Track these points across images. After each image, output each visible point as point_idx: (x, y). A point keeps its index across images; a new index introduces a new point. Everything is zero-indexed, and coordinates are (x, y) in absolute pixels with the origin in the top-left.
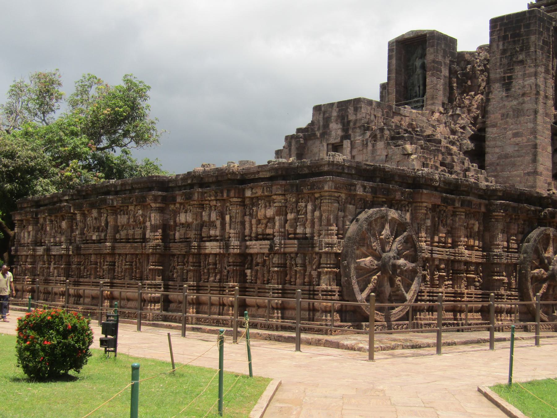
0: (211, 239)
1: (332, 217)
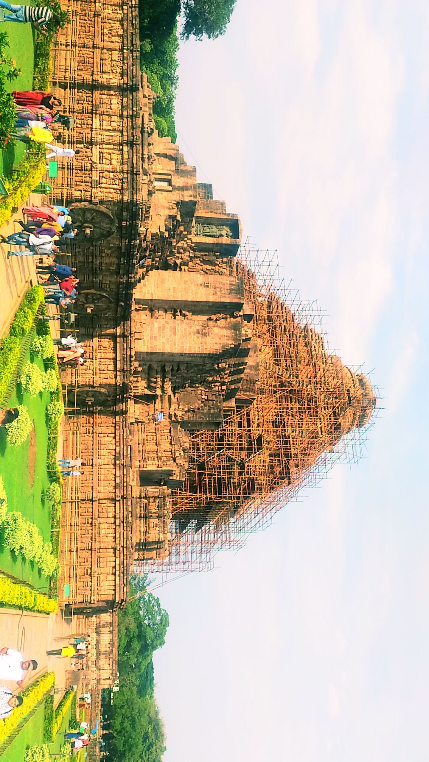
1: (110, 199)
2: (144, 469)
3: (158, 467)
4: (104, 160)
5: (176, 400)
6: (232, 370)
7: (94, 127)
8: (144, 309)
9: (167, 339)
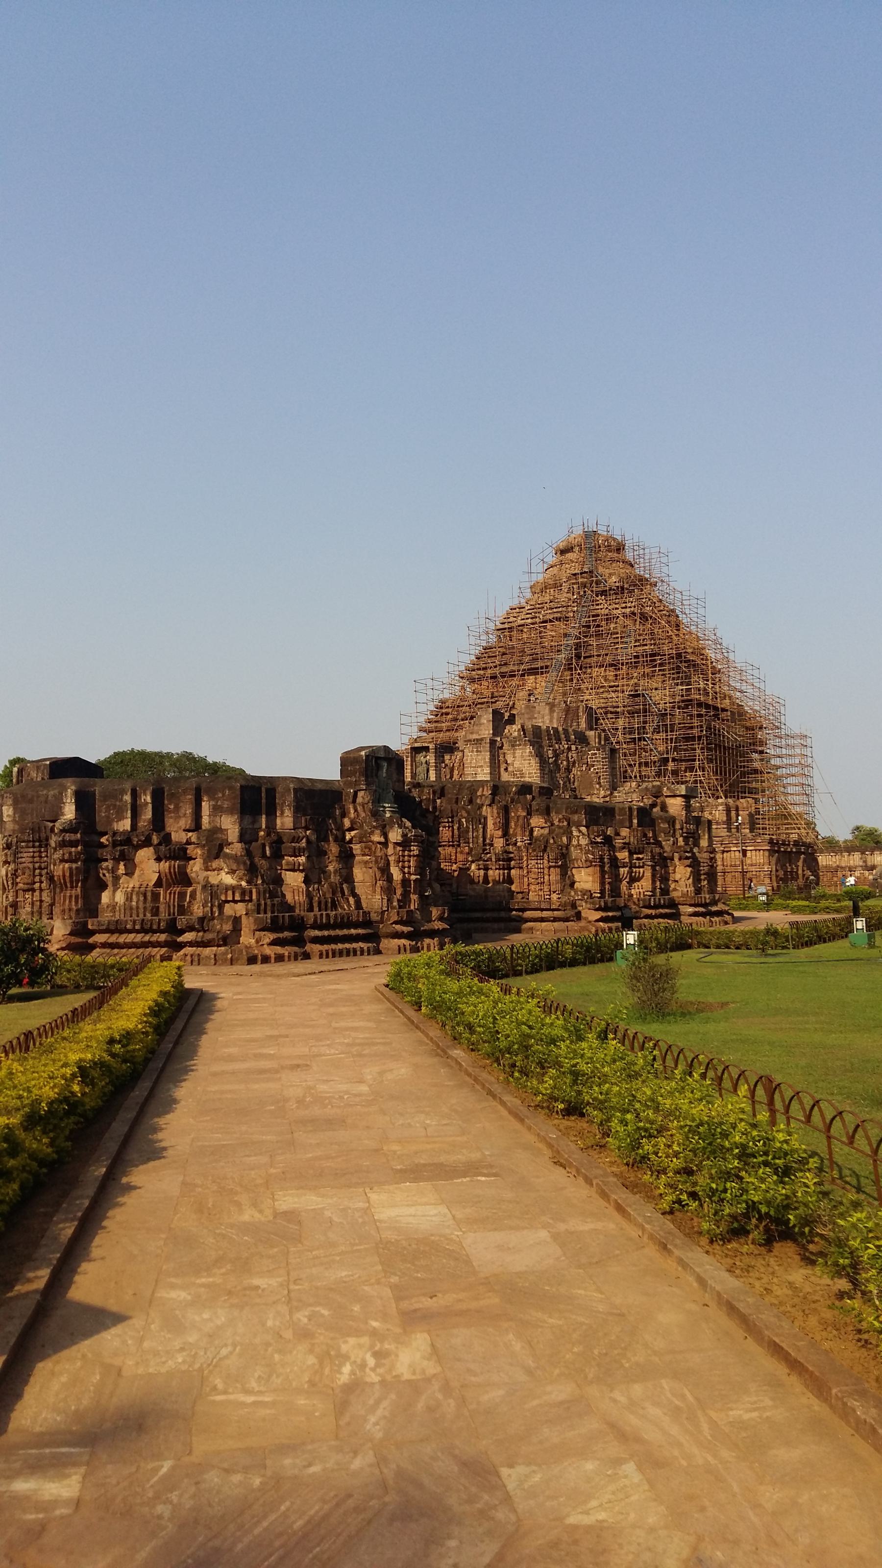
5: (589, 797)
6: (554, 742)
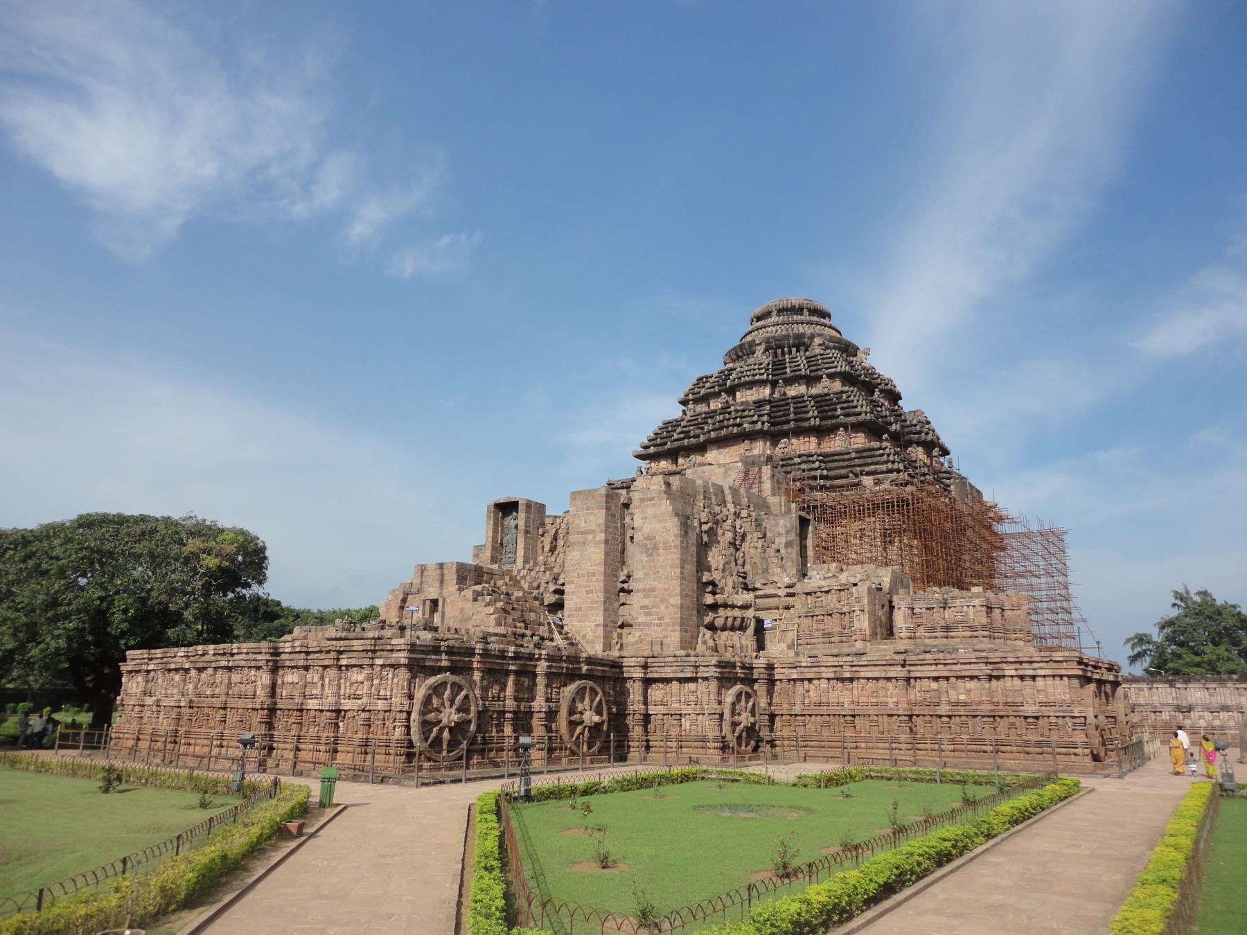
0: (312, 697)
1: (405, 683)
2: (868, 632)
3: (863, 611)
4: (358, 692)
7: (317, 707)
8: (620, 636)
9: (662, 600)
